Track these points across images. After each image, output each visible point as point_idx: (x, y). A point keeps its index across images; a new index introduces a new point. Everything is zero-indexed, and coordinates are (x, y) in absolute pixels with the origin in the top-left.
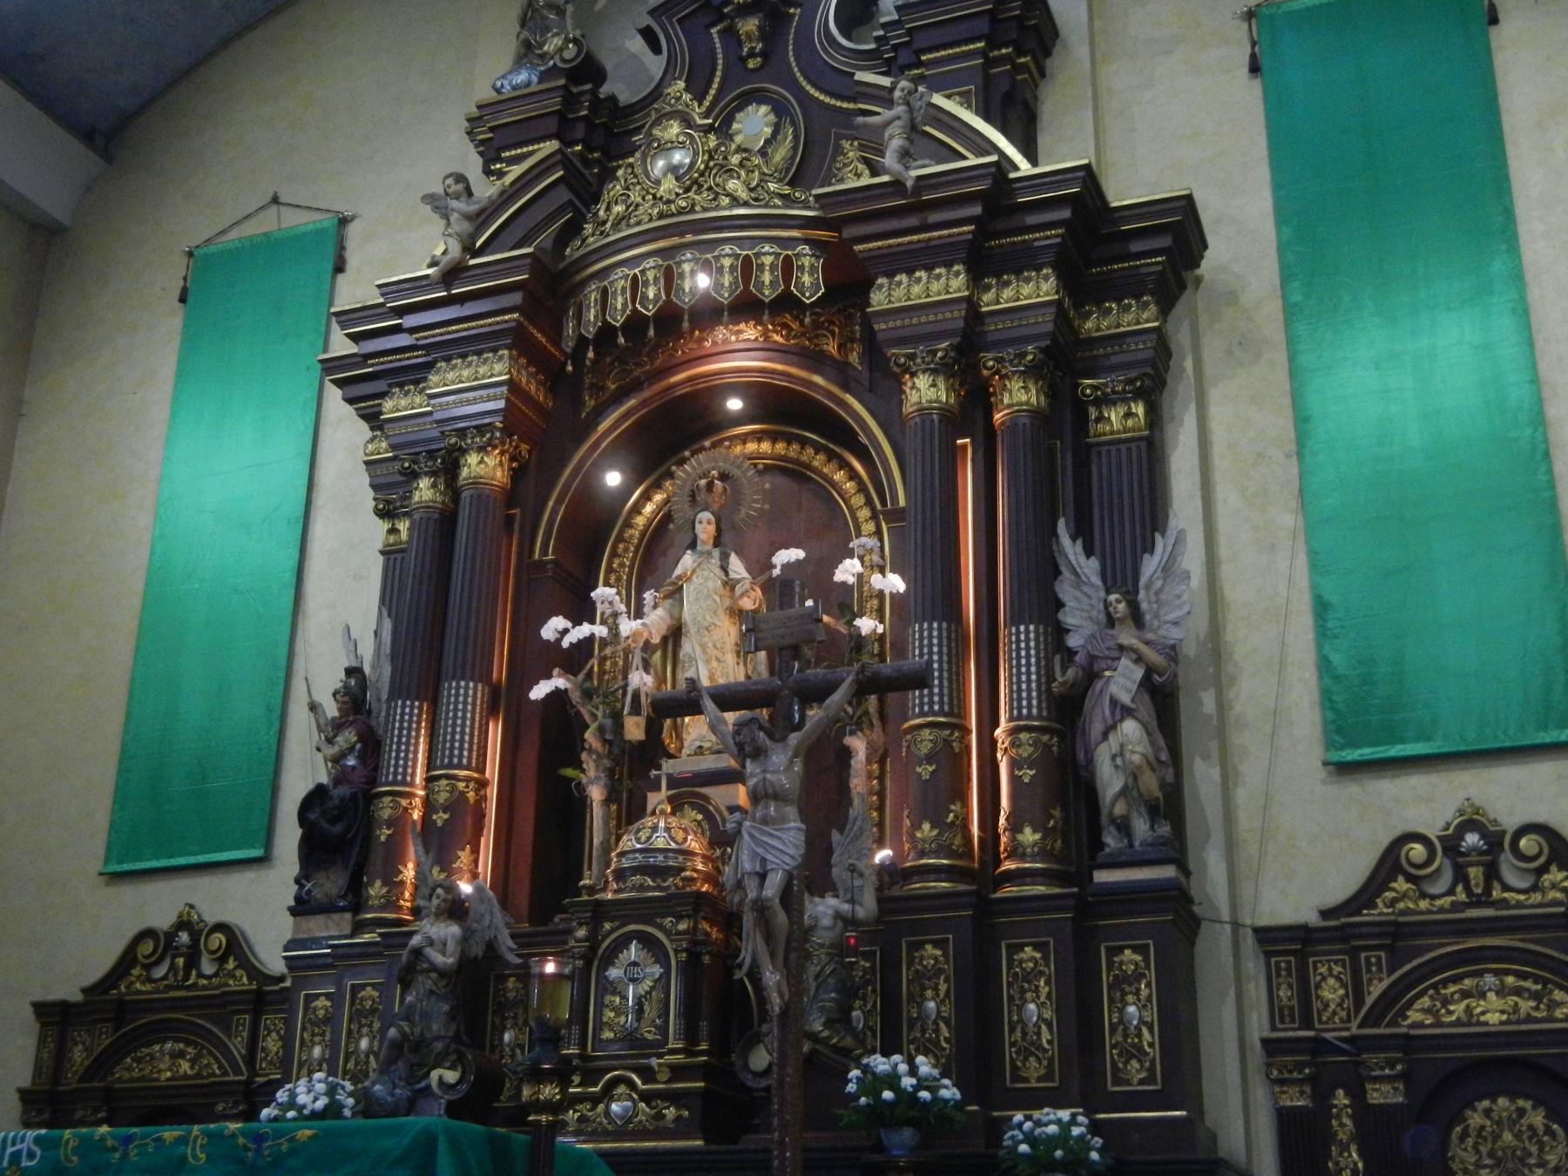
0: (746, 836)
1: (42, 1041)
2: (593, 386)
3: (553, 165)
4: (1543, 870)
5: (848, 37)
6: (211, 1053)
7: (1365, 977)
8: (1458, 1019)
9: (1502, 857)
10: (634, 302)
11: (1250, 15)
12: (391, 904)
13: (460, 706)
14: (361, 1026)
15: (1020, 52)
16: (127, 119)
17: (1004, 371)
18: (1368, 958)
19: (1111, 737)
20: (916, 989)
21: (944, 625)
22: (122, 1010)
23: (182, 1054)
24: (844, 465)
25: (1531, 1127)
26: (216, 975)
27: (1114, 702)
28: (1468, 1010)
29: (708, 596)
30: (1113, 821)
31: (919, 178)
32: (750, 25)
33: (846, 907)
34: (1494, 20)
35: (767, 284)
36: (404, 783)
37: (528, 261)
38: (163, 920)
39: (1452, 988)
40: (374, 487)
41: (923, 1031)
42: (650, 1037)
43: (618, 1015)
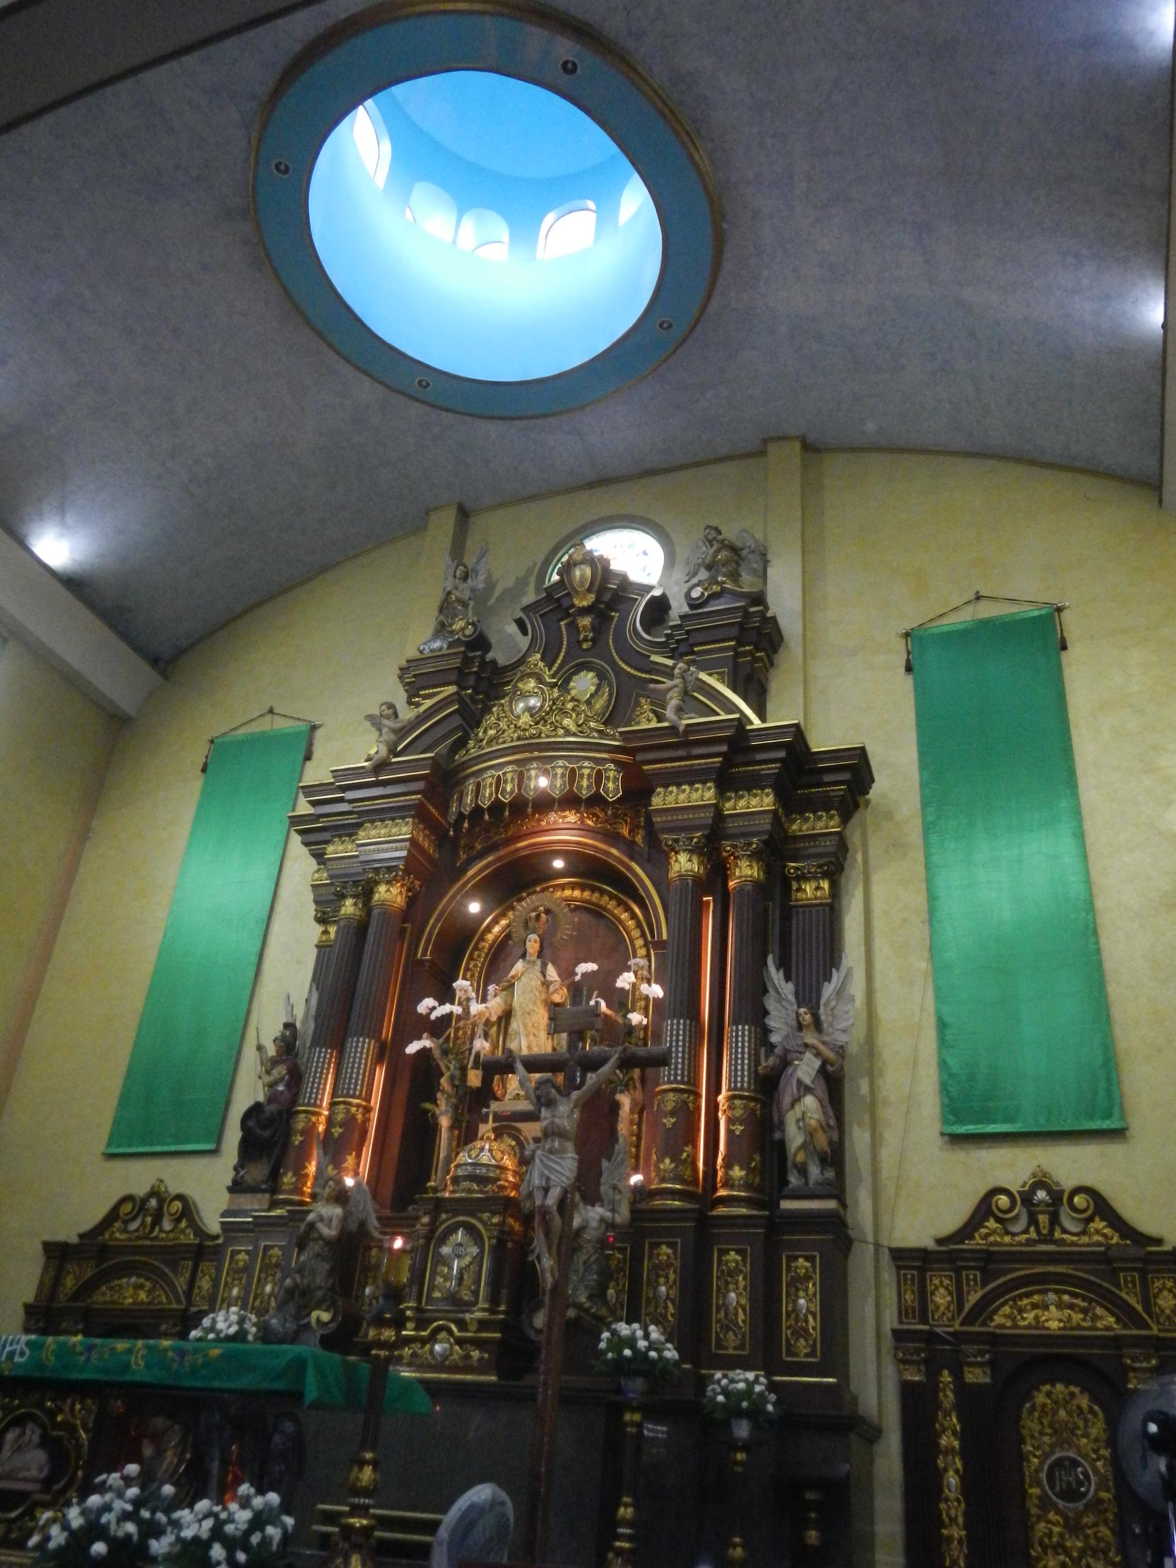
0: (537, 1161)
1: (45, 1270)
2: (466, 845)
3: (452, 701)
4: (1090, 1219)
5: (648, 633)
6: (161, 1287)
7: (965, 1289)
8: (1029, 1324)
9: (1062, 1209)
10: (497, 793)
11: (907, 635)
12: (298, 1190)
13: (358, 1055)
14: (267, 1275)
15: (758, 649)
16: (179, 653)
17: (737, 854)
18: (967, 1276)
19: (797, 1107)
20: (653, 1277)
21: (688, 1022)
22: (104, 1251)
23: (141, 1287)
24: (628, 909)
25: (1079, 1407)
26: (172, 1231)
27: (800, 1083)
28: (1036, 1318)
29: (532, 991)
30: (795, 1165)
31: (688, 725)
32: (585, 621)
33: (608, 1214)
34: (1064, 647)
35: (585, 787)
36: (315, 1105)
37: (430, 762)
38: (141, 1190)
39: (1025, 1301)
40: (316, 902)
41: (656, 1307)
42: (466, 1298)
43: (445, 1281)
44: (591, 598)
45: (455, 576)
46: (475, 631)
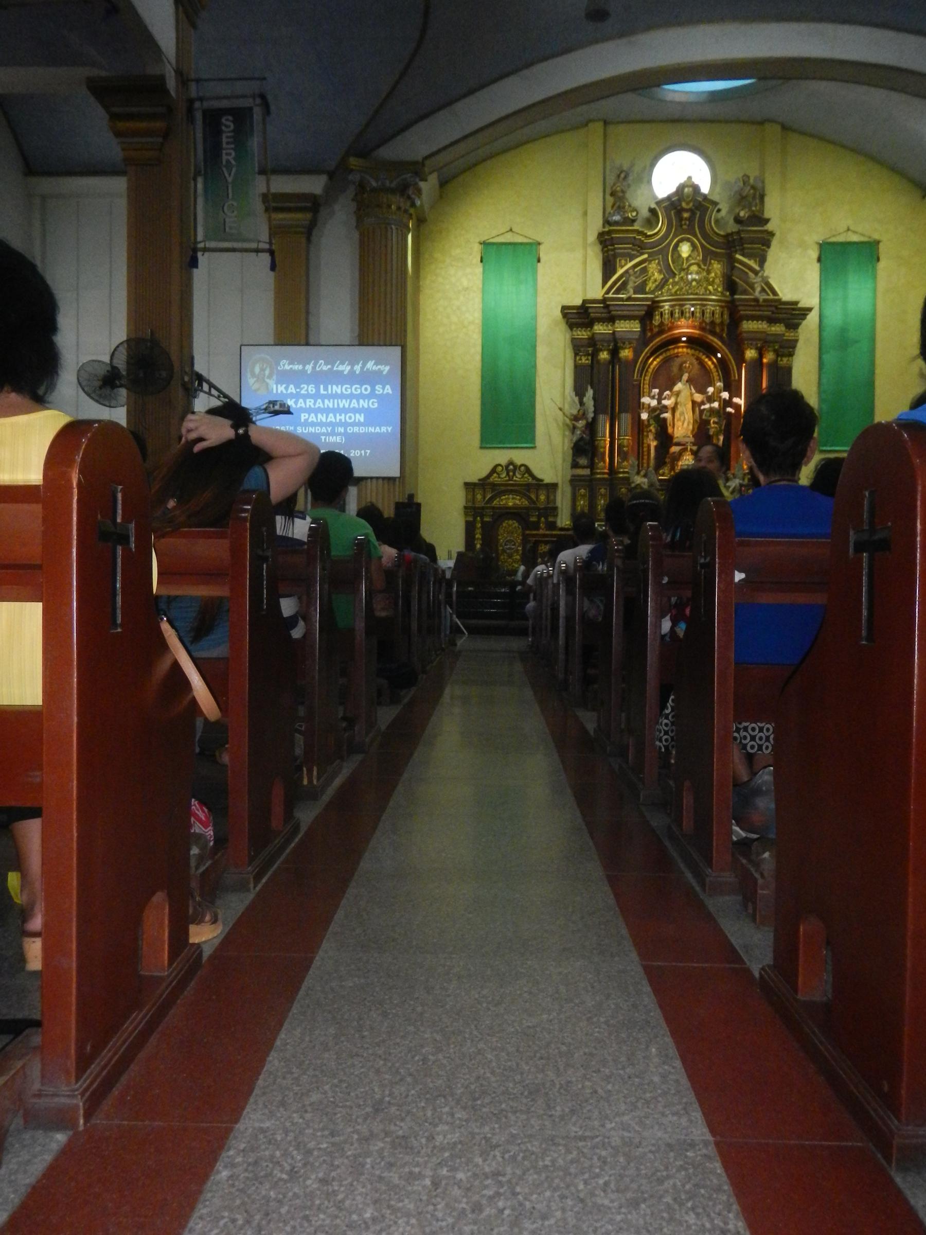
22: (494, 485)
24: (710, 359)
32: (686, 215)
33: (741, 482)
34: (878, 260)
38: (503, 461)
44: (691, 204)
45: (619, 176)
46: (637, 213)
